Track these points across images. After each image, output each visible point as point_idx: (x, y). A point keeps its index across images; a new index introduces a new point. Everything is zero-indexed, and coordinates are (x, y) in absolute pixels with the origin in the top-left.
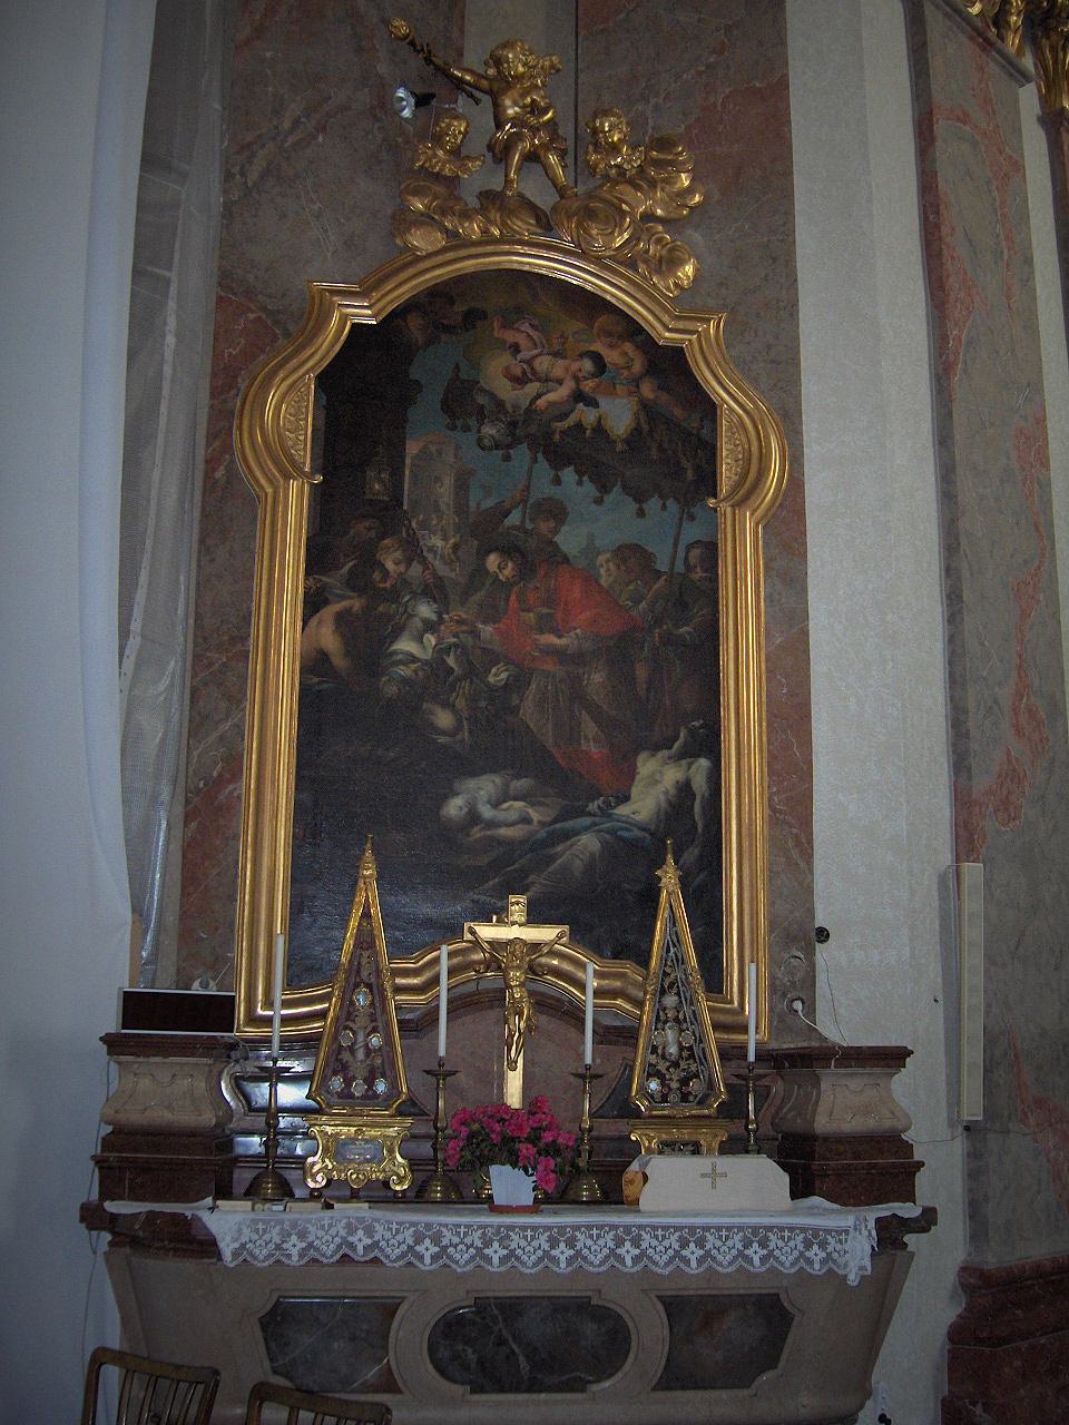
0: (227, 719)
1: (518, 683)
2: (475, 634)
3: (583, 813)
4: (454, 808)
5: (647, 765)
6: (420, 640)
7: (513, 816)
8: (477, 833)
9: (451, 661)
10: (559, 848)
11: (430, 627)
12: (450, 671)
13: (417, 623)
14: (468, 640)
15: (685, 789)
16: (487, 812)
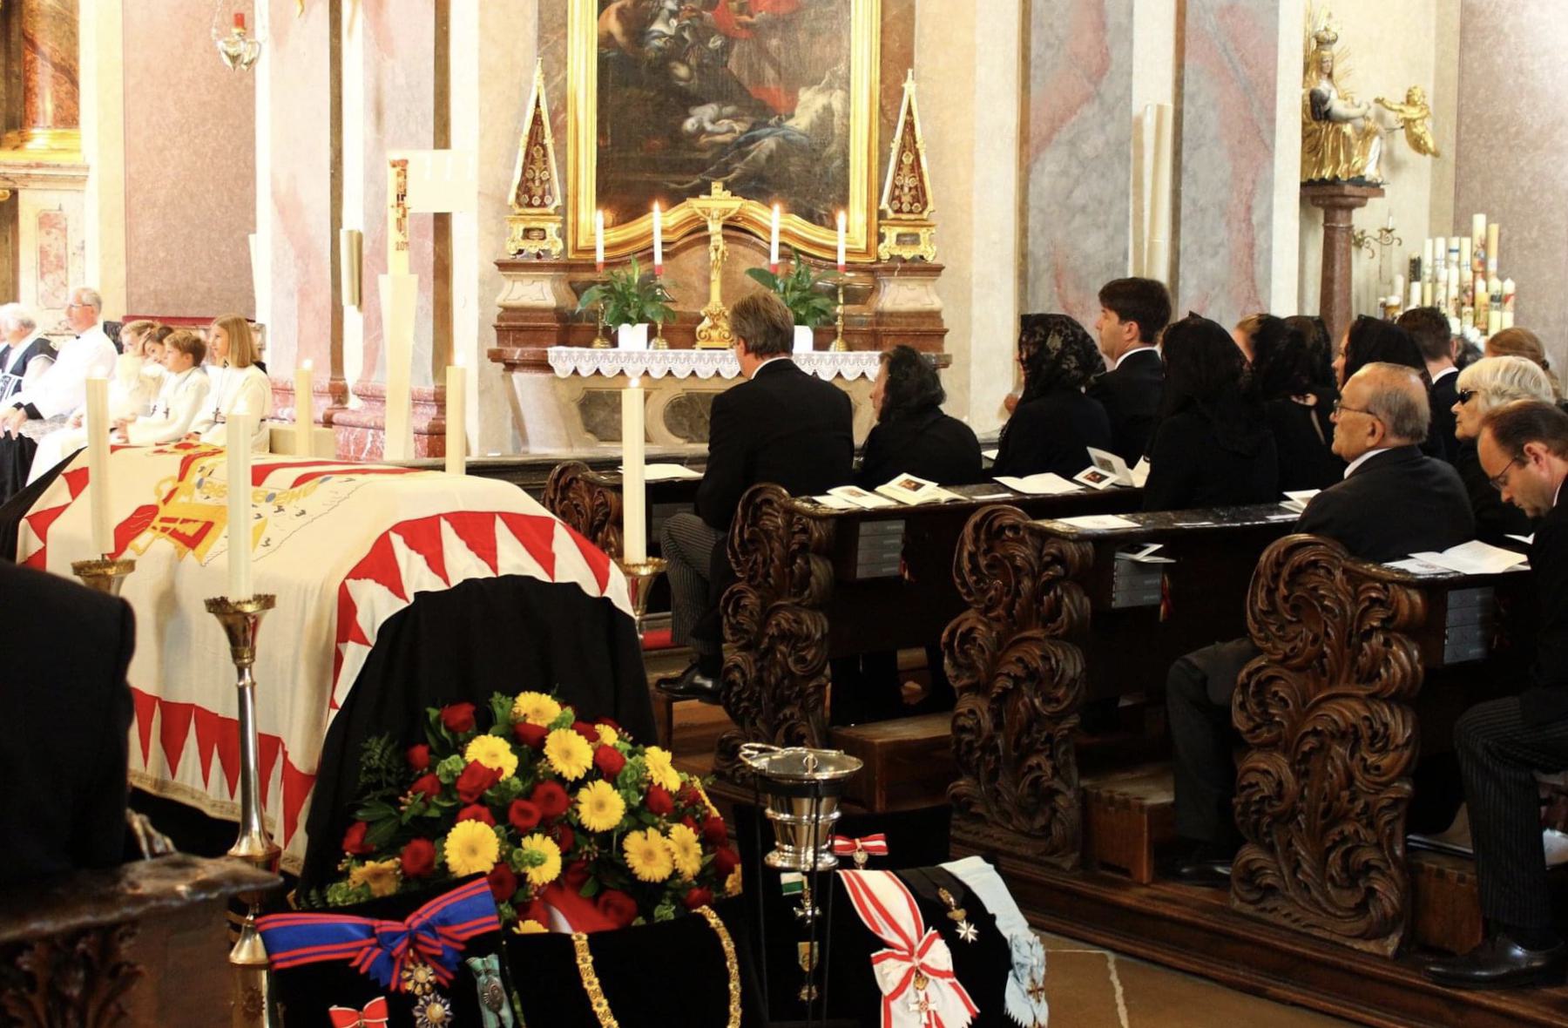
0: (558, 74)
1: (726, 49)
2: (701, 18)
3: (766, 125)
4: (690, 125)
5: (805, 95)
6: (667, 23)
7: (725, 128)
8: (703, 139)
9: (686, 35)
10: (752, 147)
11: (673, 14)
12: (685, 41)
13: (665, 13)
14: (697, 23)
15: (828, 109)
16: (709, 127)
